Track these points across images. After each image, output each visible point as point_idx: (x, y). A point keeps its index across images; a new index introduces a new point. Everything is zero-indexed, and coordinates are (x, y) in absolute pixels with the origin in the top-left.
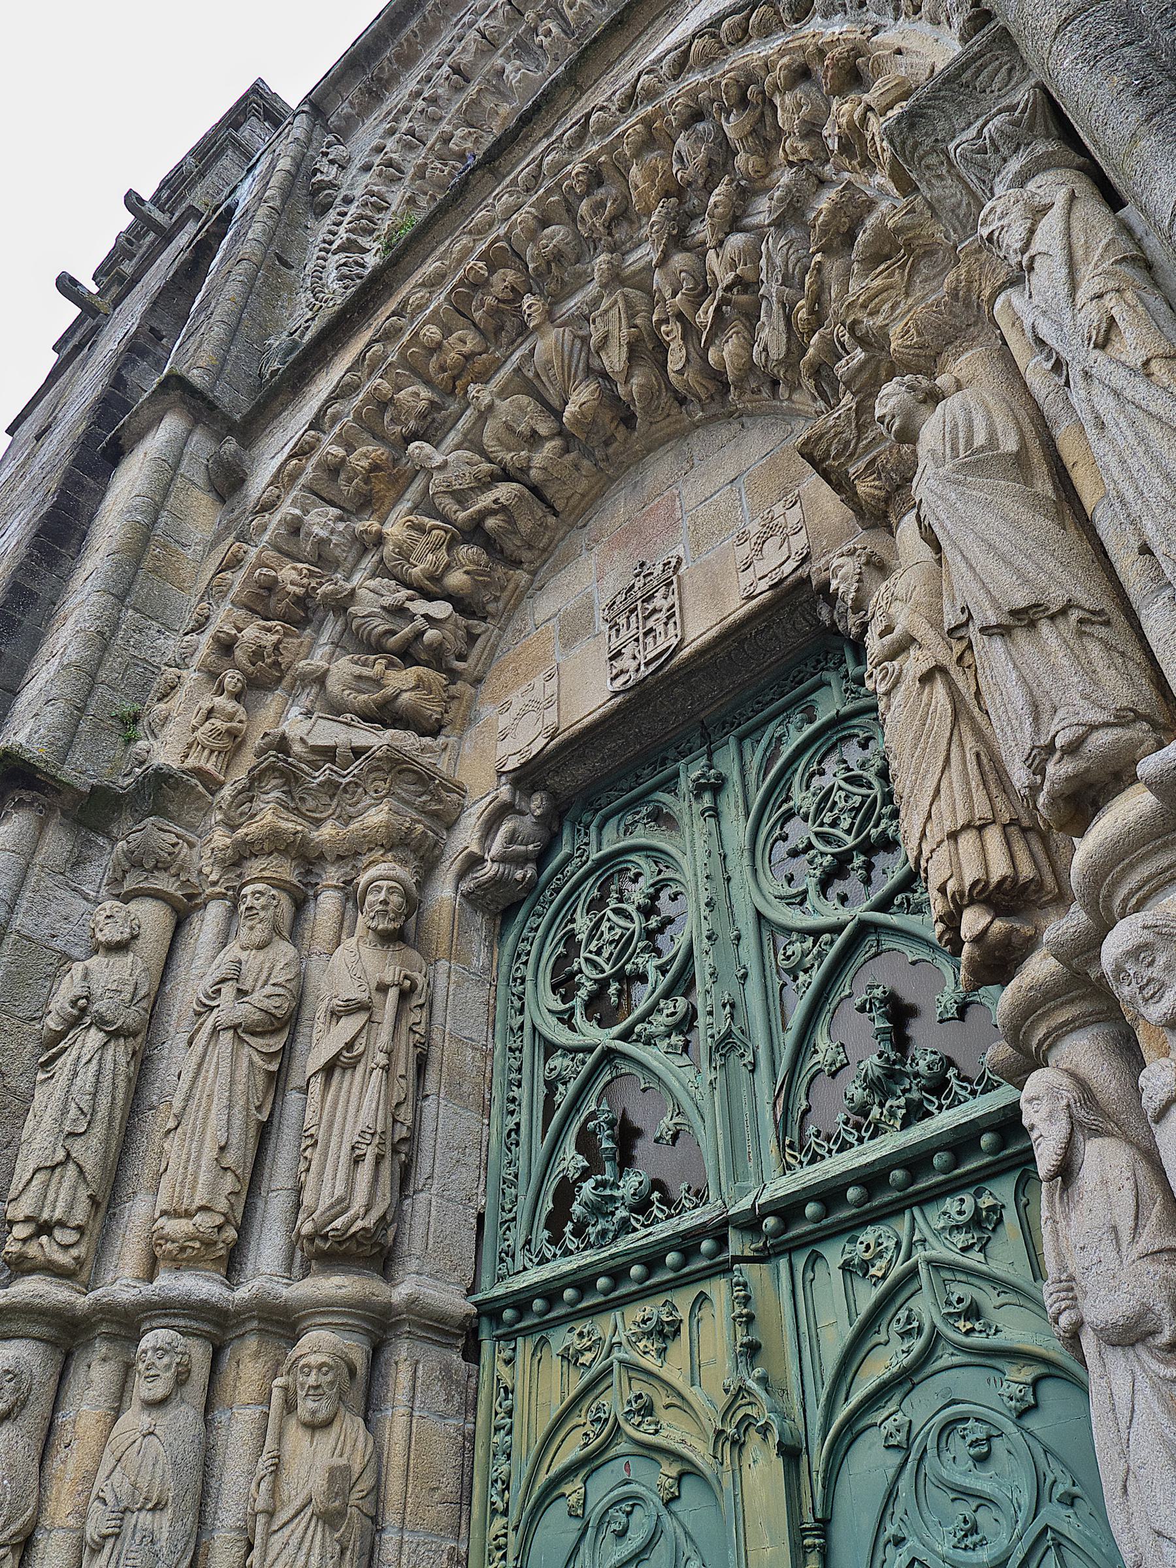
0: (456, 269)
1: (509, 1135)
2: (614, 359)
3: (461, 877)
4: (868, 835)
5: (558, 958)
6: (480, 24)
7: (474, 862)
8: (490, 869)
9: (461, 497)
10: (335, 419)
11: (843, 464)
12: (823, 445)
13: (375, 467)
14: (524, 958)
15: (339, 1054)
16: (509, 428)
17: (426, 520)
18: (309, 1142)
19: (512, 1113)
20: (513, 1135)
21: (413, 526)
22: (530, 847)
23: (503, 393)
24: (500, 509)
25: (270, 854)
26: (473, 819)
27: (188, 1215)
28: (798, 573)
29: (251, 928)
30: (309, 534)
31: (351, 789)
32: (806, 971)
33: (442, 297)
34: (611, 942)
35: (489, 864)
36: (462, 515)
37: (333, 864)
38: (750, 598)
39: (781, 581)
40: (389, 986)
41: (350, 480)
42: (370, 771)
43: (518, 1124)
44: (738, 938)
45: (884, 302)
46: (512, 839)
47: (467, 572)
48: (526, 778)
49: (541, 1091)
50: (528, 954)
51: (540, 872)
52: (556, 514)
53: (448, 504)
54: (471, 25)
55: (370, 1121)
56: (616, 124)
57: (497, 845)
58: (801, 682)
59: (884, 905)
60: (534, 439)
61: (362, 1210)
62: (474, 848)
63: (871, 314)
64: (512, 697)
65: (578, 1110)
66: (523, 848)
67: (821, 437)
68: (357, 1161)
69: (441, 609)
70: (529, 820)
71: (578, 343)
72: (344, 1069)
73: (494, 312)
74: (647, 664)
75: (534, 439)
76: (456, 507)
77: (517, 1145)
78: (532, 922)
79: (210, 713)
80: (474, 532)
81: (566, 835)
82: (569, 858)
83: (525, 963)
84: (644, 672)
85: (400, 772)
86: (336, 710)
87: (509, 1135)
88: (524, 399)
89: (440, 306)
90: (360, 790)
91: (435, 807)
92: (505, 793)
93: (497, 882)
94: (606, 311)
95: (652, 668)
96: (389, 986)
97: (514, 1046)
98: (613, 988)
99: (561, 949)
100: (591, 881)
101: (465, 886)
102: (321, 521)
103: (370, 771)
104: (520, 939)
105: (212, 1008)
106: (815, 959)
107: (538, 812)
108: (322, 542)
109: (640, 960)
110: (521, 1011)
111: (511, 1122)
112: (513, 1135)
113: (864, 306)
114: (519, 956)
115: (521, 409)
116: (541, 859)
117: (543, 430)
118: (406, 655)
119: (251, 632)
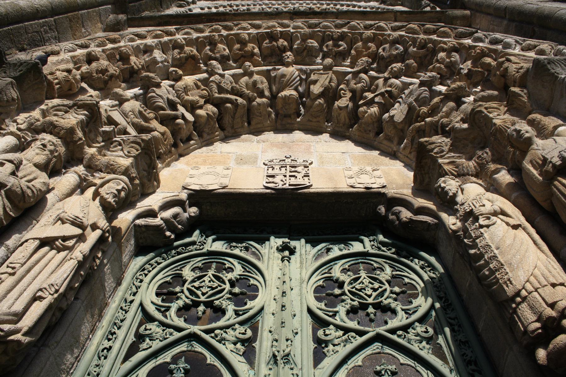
0: (265, 29)
1: (103, 351)
2: (316, 89)
3: (139, 216)
4: (381, 302)
5: (166, 282)
6: (264, 6)
7: (151, 213)
8: (157, 221)
9: (221, 90)
11: (437, 157)
12: (433, 146)
14: (146, 272)
15: (56, 238)
18: (10, 270)
19: (109, 340)
20: (105, 351)
21: (196, 84)
22: (180, 226)
25: (59, 138)
26: (161, 198)
28: (380, 189)
31: (115, 144)
32: (334, 345)
34: (209, 287)
35: (159, 219)
36: (217, 95)
37: (84, 167)
38: (352, 187)
39: (371, 188)
40: (98, 228)
42: (132, 142)
43: (111, 347)
44: (295, 316)
45: (495, 112)
46: (175, 216)
47: (207, 114)
48: (198, 197)
49: (131, 338)
50: (149, 272)
51: (176, 239)
52: (249, 123)
54: (260, 5)
55: (59, 282)
57: (168, 214)
58: (346, 234)
59: (393, 331)
60: (261, 94)
61: (25, 329)
62: (156, 208)
63: (488, 112)
64: (202, 167)
65: (156, 357)
66: (177, 224)
67: (434, 143)
68: (35, 299)
69: (190, 117)
70: (186, 215)
71: (298, 78)
72: (52, 249)
73: (272, 49)
74: (290, 185)
75: (261, 94)
76: (217, 91)
77: (106, 358)
78: (158, 259)
79: (69, 71)
80: (218, 104)
81: (197, 232)
82: (194, 243)
83: (146, 275)
84: (287, 186)
85: (146, 153)
86: (125, 115)
87: (103, 351)
89: (252, 33)
90: (120, 147)
91: (145, 181)
92: (184, 196)
93: (157, 228)
94: (322, 74)
96: (98, 228)
97: (124, 308)
98: (201, 308)
99: (168, 279)
100: (200, 259)
101: (138, 222)
103: (132, 142)
104: (147, 262)
106: (342, 341)
107: (193, 214)
109: (224, 302)
110: (134, 294)
111: (107, 344)
112: (105, 351)
113: (486, 108)
114: (144, 270)
115: (262, 83)
116: (180, 235)
117: (267, 93)
118: (163, 121)
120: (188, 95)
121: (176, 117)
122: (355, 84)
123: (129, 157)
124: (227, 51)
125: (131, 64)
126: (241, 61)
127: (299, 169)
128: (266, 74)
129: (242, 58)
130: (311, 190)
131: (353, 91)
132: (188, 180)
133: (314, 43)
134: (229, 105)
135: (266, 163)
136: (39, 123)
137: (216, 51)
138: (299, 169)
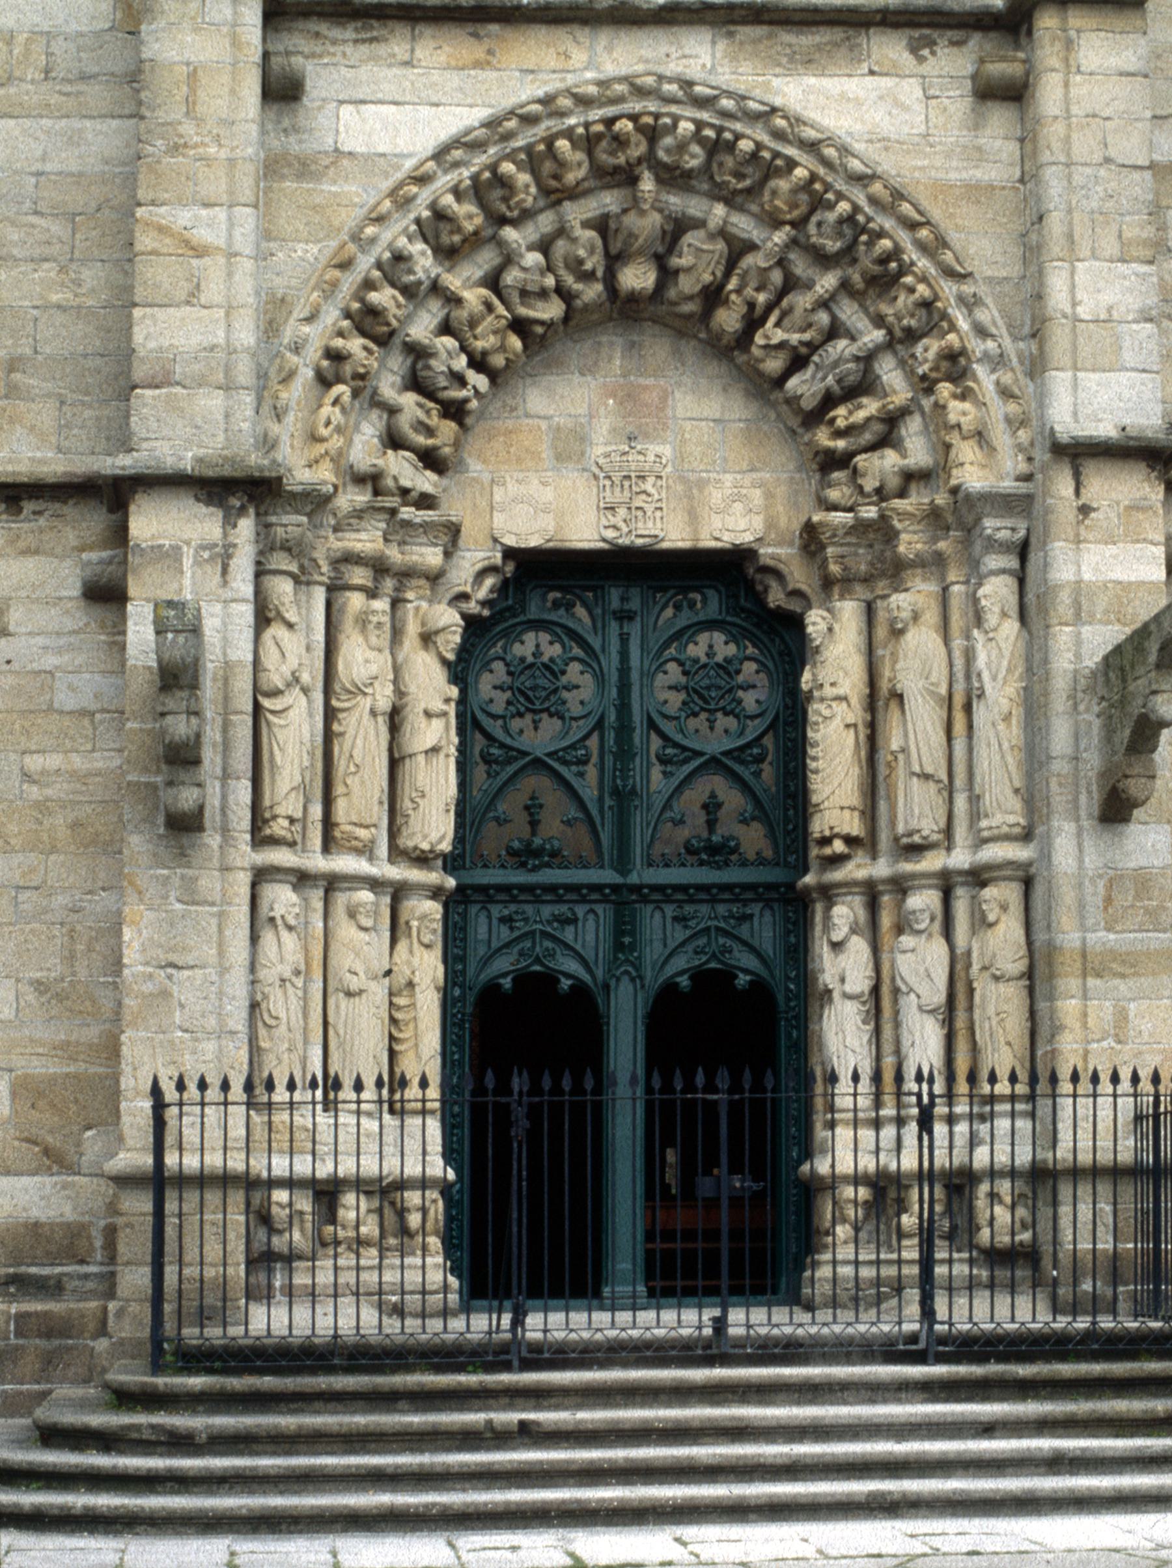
2: (687, 285)
8: (473, 607)
9: (524, 293)
10: (456, 165)
13: (476, 233)
16: (581, 262)
17: (496, 302)
23: (586, 224)
24: (549, 325)
27: (367, 827)
29: (378, 636)
30: (411, 271)
33: (582, 120)
41: (452, 232)
46: (491, 591)
53: (515, 298)
56: (789, 142)
70: (501, 577)
74: (637, 536)
88: (599, 242)
92: (498, 558)
95: (640, 542)
102: (424, 263)
105: (365, 694)
108: (419, 283)
119: (355, 345)
120: (475, 338)
121: (466, 401)
122: (758, 289)
123: (436, 545)
124: (533, 190)
125: (388, 324)
126: (553, 197)
127: (648, 486)
128: (602, 225)
129: (556, 194)
130: (665, 545)
131: (751, 305)
132: (499, 520)
133: (695, 158)
134: (539, 330)
135: (601, 461)
136: (339, 554)
137: (512, 203)
138: (648, 486)
